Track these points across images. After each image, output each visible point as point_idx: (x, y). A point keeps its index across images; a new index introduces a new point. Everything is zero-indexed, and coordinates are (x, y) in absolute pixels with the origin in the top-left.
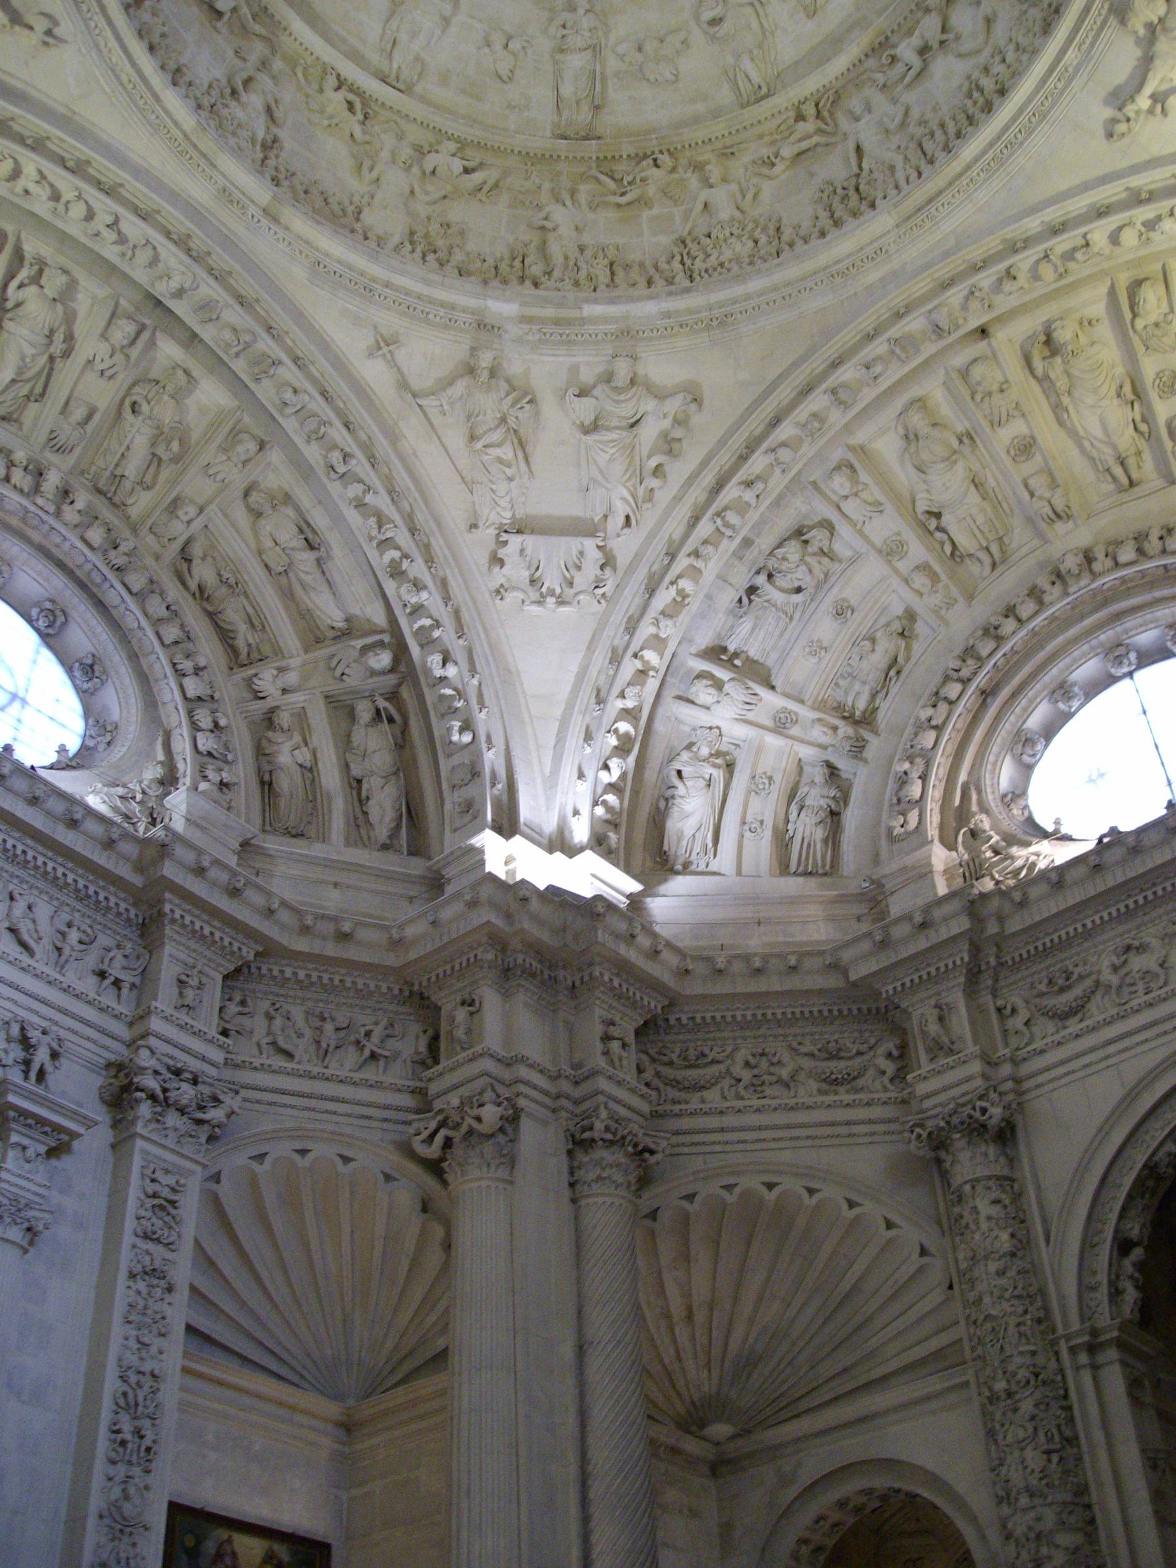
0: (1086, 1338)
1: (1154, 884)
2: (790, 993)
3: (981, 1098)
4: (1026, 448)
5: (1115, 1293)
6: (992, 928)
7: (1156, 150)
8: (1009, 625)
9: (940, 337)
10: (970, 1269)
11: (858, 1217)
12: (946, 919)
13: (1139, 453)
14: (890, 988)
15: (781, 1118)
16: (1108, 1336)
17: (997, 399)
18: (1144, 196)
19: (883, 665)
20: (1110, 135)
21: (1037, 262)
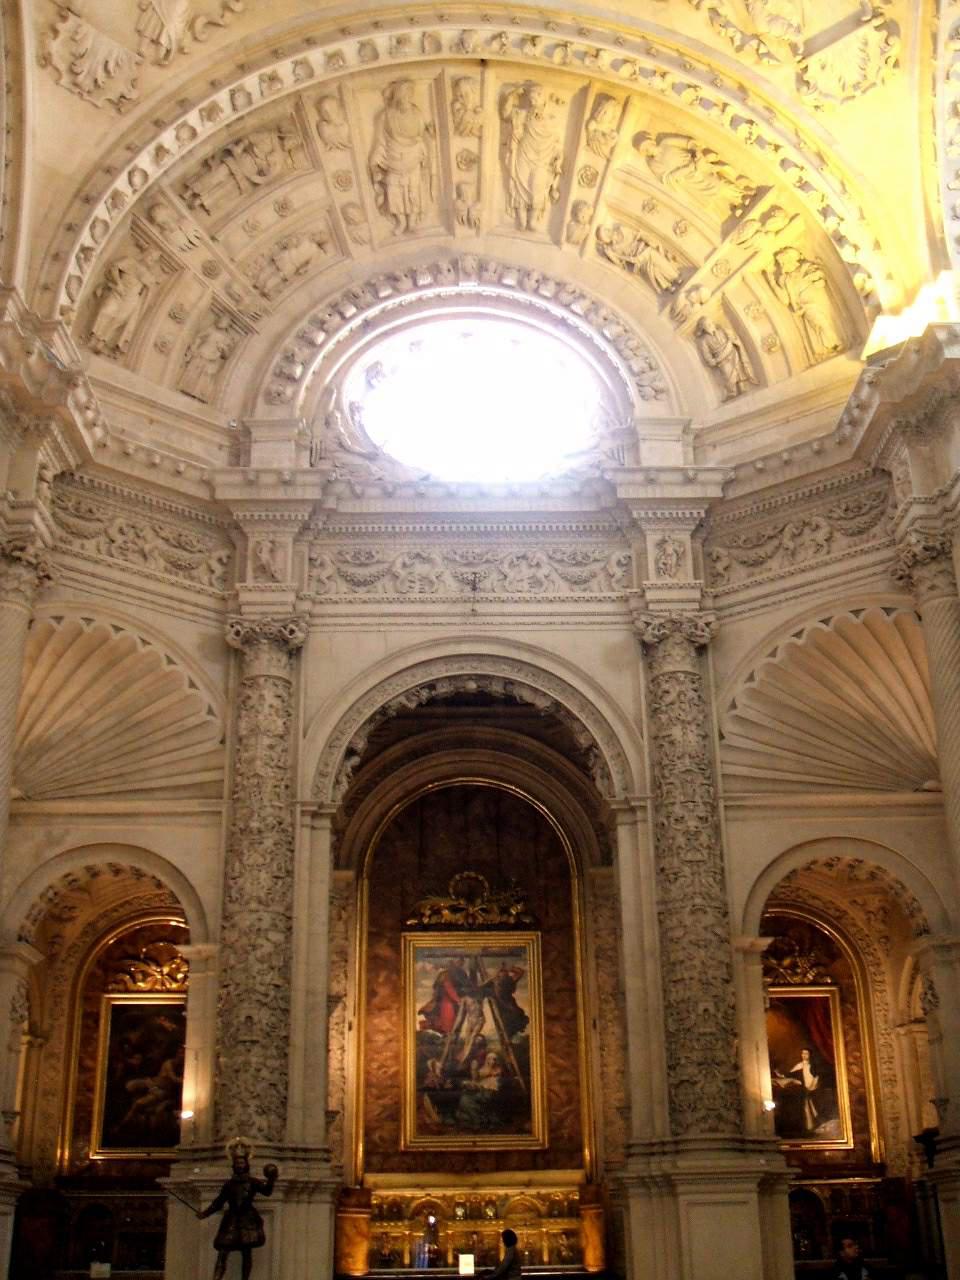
0: (315, 808)
1: (453, 522)
2: (169, 490)
3: (293, 622)
5: (337, 782)
6: (331, 503)
8: (407, 283)
9: (458, 51)
10: (247, 737)
11: (172, 672)
12: (305, 485)
13: (543, 210)
14: (241, 515)
15: (136, 581)
16: (329, 811)
18: (653, 51)
19: (303, 260)
21: (558, 46)
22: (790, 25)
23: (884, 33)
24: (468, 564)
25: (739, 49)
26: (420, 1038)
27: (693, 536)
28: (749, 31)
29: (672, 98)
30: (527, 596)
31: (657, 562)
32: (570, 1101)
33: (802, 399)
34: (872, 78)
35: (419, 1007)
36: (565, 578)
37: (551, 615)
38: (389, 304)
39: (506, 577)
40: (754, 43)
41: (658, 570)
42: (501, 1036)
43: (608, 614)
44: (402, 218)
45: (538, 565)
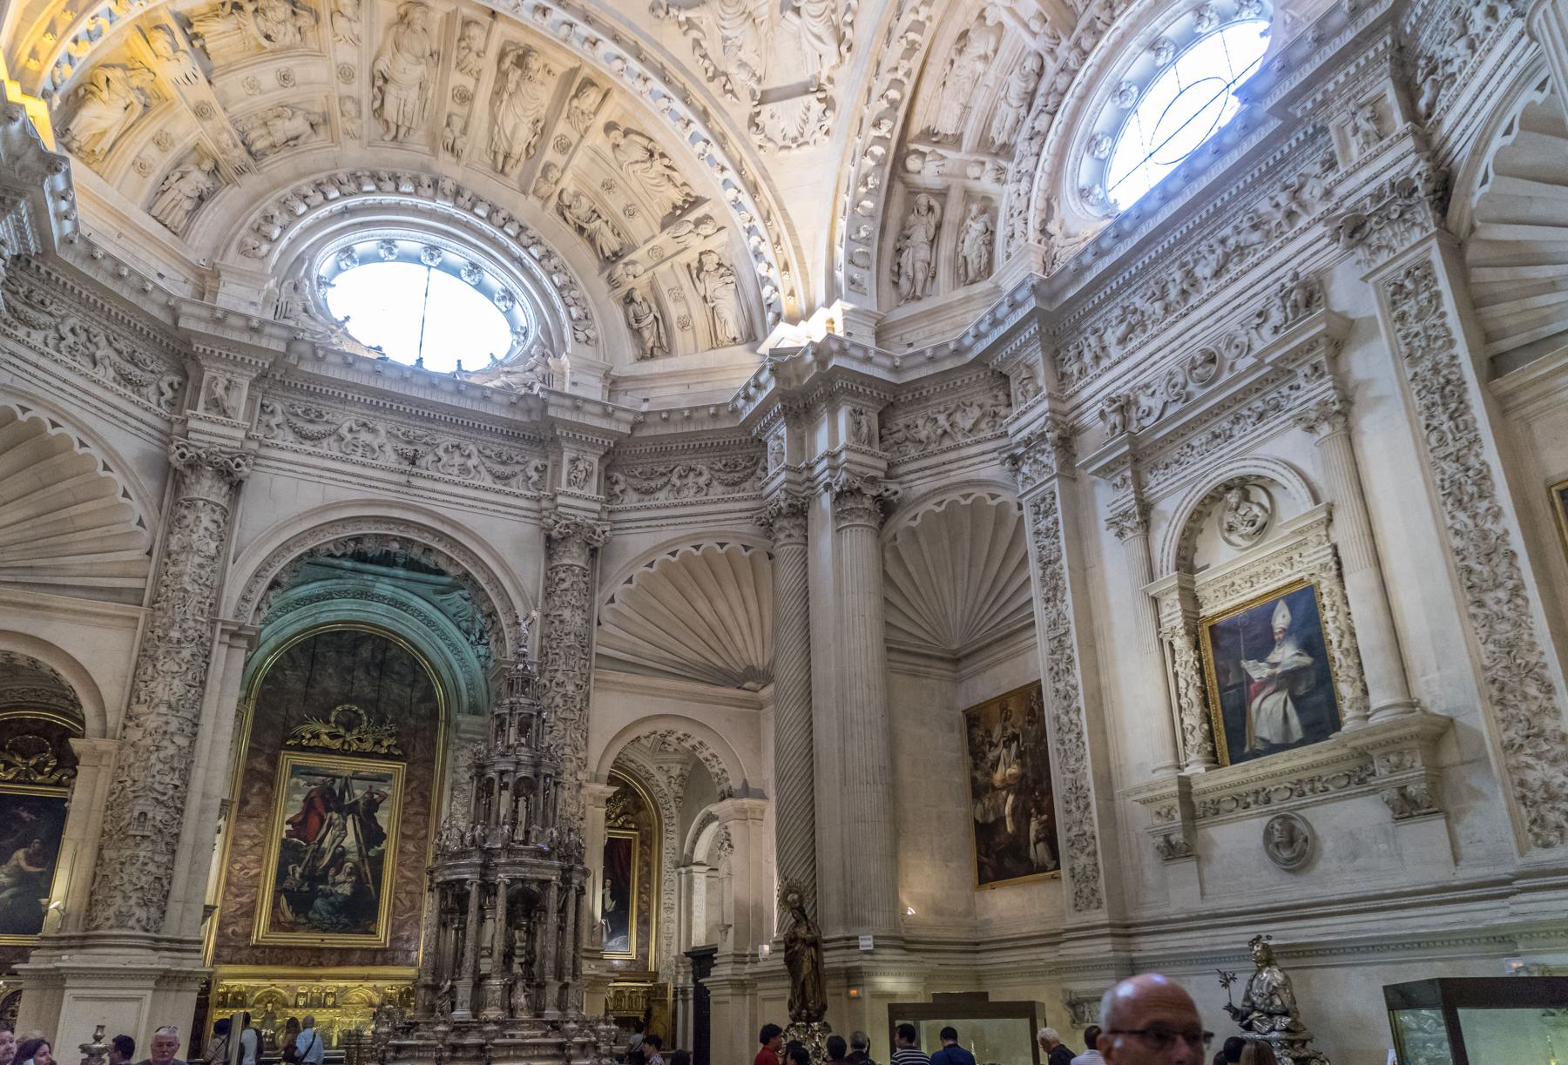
4: (465, 97)
7: (665, 42)
8: (390, 186)
17: (472, 57)
19: (291, 134)
20: (652, 9)
22: (754, 75)
23: (824, 106)
24: (409, 443)
25: (711, 79)
26: (285, 844)
27: (602, 459)
28: (721, 68)
29: (648, 101)
30: (457, 479)
31: (569, 474)
32: (413, 908)
33: (705, 372)
34: (807, 137)
35: (288, 817)
36: (490, 472)
37: (475, 499)
38: (370, 199)
39: (440, 460)
40: (724, 79)
41: (569, 483)
42: (360, 849)
43: (521, 508)
44: (393, 128)
45: (469, 456)
